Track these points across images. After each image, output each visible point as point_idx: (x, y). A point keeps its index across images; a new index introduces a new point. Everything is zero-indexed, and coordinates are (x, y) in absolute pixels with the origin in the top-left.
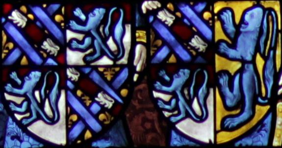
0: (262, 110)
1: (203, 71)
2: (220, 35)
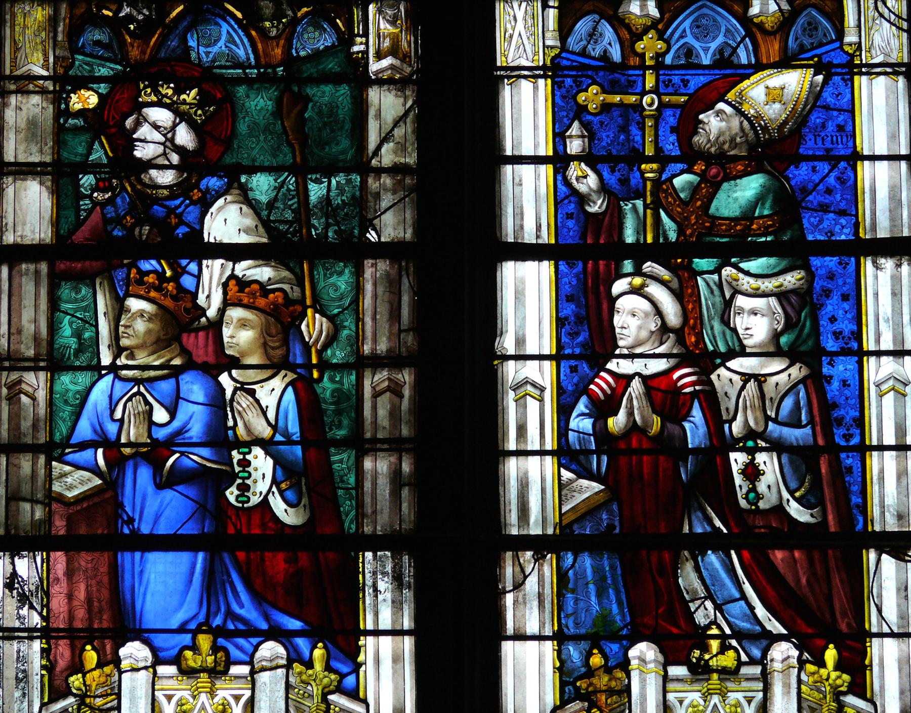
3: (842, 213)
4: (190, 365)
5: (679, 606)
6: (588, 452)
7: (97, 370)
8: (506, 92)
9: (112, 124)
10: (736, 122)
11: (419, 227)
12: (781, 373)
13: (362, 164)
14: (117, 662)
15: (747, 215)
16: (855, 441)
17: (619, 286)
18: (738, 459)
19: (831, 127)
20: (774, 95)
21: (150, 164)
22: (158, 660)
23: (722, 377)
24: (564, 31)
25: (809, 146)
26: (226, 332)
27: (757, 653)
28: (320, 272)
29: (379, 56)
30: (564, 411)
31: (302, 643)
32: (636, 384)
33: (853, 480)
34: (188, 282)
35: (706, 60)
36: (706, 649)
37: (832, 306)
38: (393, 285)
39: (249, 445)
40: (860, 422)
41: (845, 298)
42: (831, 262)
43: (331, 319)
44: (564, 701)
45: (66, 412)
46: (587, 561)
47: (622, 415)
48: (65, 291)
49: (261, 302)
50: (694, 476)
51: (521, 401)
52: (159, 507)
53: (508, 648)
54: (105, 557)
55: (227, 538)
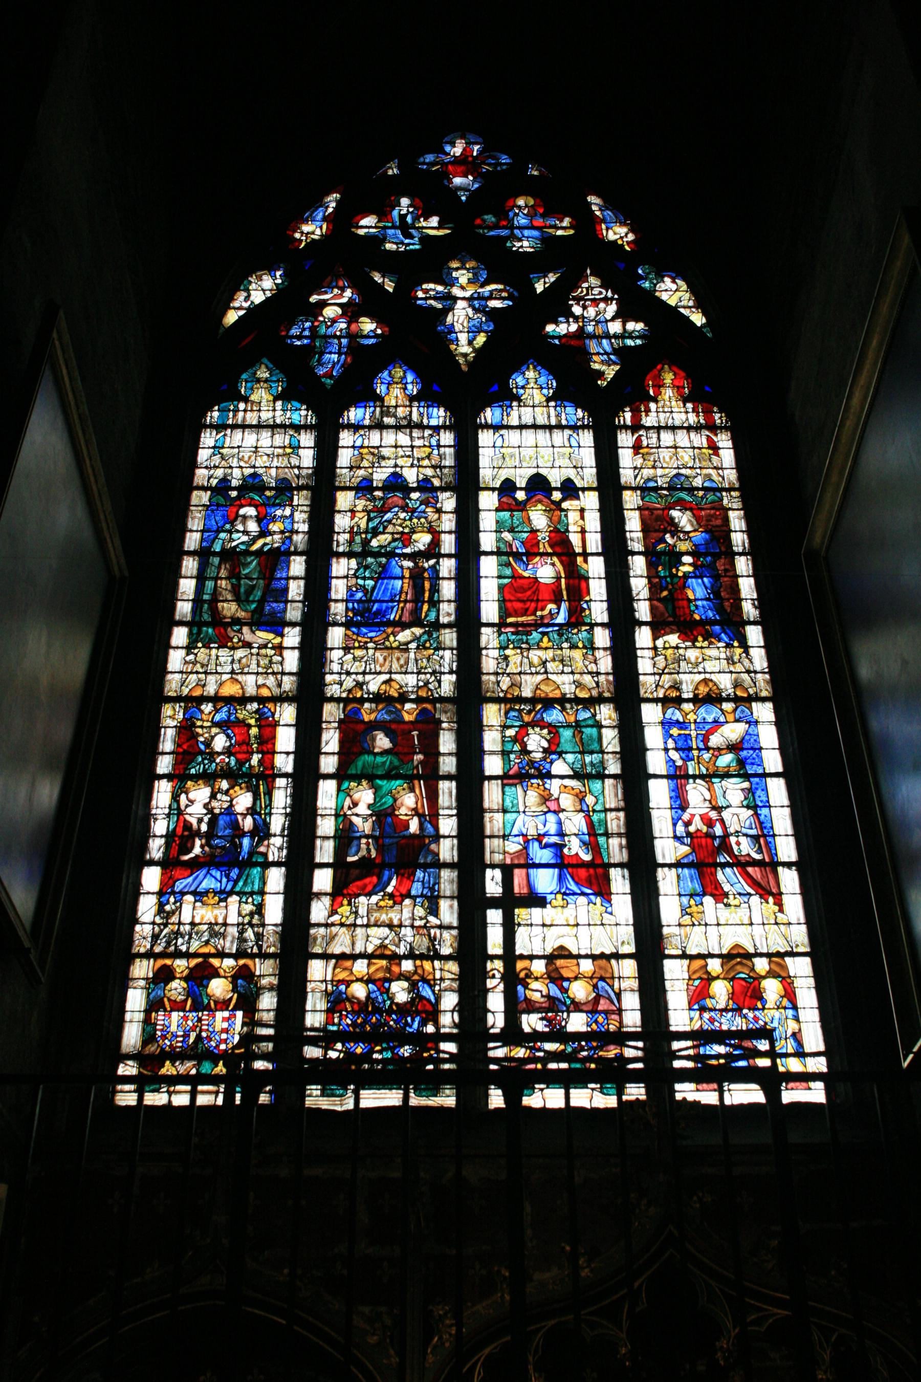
2: (767, 1020)
3: (759, 765)
4: (549, 811)
5: (718, 886)
7: (519, 812)
10: (722, 738)
11: (623, 769)
13: (602, 752)
15: (729, 766)
17: (688, 787)
18: (733, 840)
20: (733, 731)
23: (726, 814)
25: (746, 745)
28: (590, 783)
30: (675, 825)
31: (592, 897)
33: (772, 845)
34: (547, 786)
36: (728, 898)
37: (759, 793)
38: (616, 787)
40: (772, 828)
42: (757, 780)
45: (509, 826)
46: (686, 871)
48: (507, 789)
49: (572, 792)
50: (720, 845)
55: (563, 864)
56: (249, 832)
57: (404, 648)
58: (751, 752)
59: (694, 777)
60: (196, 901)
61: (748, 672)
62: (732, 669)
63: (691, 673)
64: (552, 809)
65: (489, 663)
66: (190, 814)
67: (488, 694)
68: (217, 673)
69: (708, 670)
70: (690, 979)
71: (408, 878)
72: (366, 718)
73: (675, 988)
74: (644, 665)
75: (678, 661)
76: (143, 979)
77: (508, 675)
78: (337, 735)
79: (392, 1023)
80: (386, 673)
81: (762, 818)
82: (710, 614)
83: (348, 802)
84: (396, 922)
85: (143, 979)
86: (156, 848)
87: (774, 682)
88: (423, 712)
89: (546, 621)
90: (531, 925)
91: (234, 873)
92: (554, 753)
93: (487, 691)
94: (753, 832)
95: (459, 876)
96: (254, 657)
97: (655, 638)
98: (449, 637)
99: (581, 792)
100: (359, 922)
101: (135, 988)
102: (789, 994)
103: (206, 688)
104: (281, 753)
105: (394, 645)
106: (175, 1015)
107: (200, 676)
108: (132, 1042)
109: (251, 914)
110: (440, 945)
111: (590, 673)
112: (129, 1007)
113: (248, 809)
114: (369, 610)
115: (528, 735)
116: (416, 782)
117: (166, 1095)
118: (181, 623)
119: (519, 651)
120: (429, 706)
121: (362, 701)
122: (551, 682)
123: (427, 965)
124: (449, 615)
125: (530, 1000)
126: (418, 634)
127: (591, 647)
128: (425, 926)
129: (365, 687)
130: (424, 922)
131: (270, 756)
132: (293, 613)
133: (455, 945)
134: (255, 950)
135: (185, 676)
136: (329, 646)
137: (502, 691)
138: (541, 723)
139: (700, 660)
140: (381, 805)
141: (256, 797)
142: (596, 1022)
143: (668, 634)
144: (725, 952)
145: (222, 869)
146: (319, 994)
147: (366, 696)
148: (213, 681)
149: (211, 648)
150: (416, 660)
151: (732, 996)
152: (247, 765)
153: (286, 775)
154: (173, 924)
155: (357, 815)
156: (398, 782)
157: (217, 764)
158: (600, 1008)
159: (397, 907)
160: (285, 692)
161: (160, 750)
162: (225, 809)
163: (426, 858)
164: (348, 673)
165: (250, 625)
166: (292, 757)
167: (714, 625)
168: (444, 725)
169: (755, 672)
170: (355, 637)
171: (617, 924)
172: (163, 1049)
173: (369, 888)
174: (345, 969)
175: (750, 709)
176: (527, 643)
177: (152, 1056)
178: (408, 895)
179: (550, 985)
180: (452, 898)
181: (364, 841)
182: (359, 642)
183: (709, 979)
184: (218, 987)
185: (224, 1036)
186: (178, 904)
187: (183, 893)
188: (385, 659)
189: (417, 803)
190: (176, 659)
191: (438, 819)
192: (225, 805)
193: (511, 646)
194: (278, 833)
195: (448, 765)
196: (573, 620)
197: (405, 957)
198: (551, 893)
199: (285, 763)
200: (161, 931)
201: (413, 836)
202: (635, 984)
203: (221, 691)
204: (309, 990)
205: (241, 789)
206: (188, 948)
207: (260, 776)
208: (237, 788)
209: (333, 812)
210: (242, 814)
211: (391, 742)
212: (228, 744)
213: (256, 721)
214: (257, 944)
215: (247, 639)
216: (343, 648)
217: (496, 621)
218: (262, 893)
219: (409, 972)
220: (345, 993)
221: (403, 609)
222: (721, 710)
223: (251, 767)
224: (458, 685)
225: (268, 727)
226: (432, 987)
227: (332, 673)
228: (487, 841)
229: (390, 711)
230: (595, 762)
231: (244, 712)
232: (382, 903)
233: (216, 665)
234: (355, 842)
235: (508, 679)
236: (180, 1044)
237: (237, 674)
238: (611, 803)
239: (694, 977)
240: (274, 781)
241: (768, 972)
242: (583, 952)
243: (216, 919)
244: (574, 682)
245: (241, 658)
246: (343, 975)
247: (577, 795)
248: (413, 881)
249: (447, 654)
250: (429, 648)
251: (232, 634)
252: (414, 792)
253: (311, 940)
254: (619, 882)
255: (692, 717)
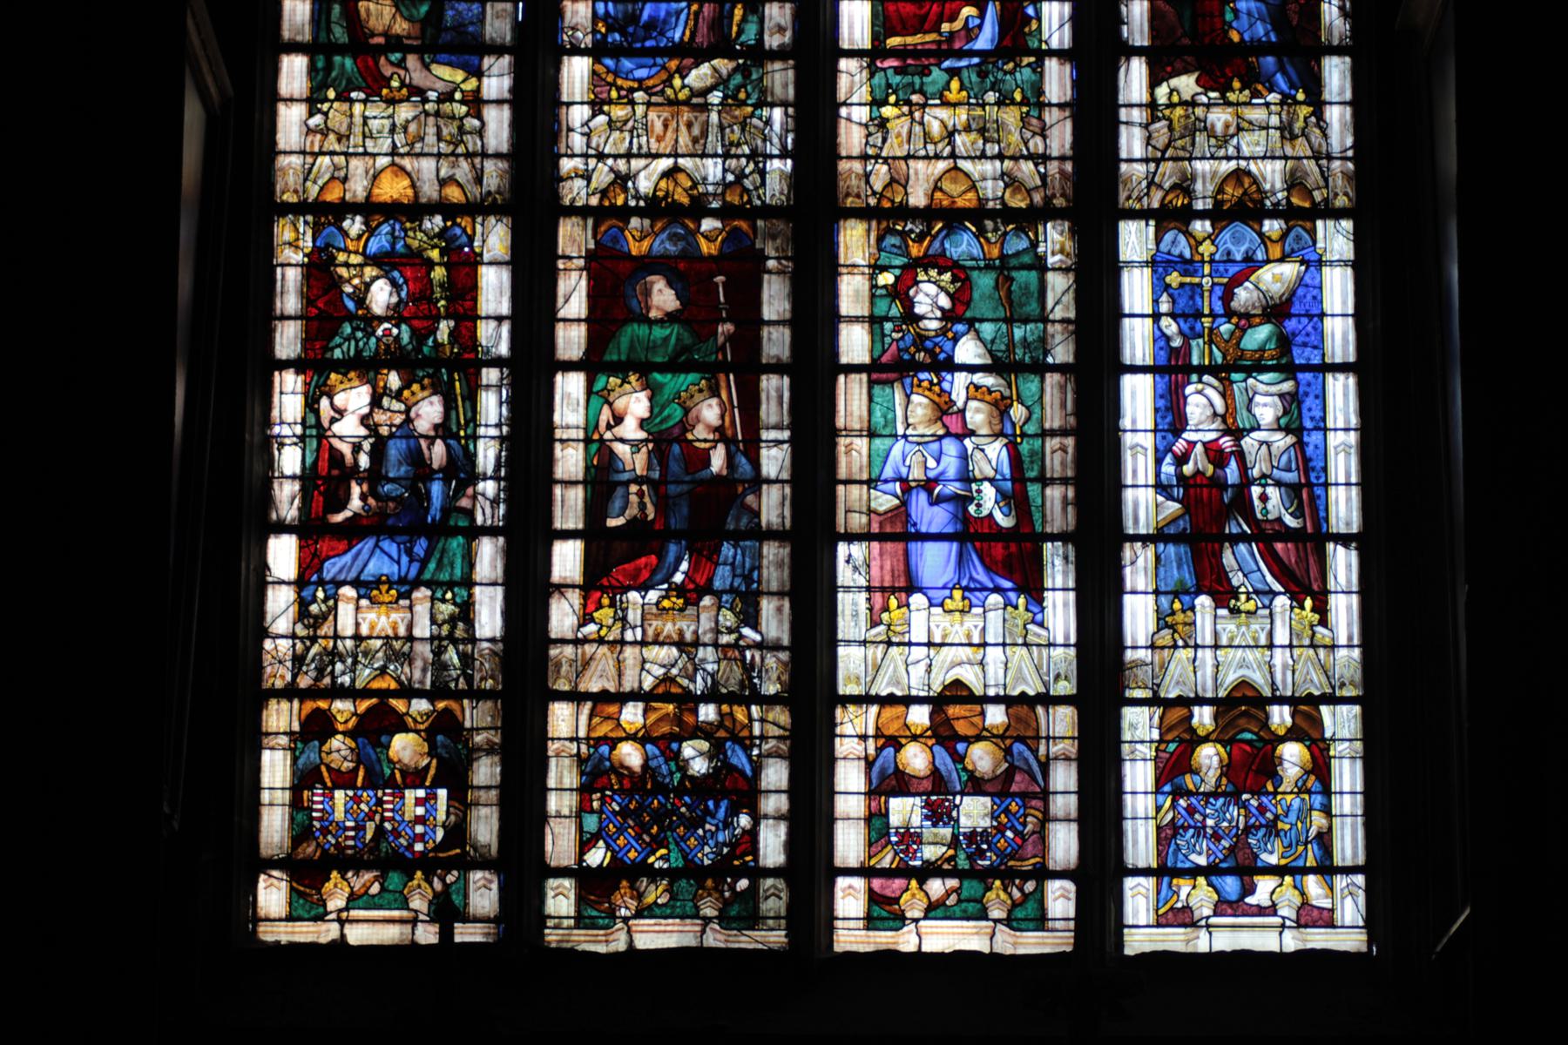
0: (1301, 848)
1: (1272, 829)
2: (1280, 811)
3: (1315, 347)
4: (948, 434)
5: (1222, 575)
6: (1171, 486)
7: (896, 436)
8: (1125, 276)
9: (901, 292)
10: (1255, 294)
11: (1077, 354)
12: (1281, 441)
13: (1044, 319)
14: (908, 605)
15: (1262, 350)
16: (1322, 480)
17: (1189, 390)
18: (1256, 491)
19: (1309, 297)
21: (922, 318)
22: (931, 605)
23: (1248, 443)
24: (1158, 240)
25: (1296, 308)
26: (968, 415)
27: (1267, 602)
28: (1020, 380)
29: (1053, 254)
30: (1159, 462)
31: (1012, 595)
32: (1199, 447)
33: (1321, 504)
34: (946, 386)
35: (1239, 257)
36: (1237, 599)
37: (1309, 402)
38: (1063, 389)
39: (982, 480)
40: (1325, 469)
41: (1317, 397)
43: (1028, 408)
44: (1159, 630)
45: (878, 462)
46: (1171, 549)
47: (1191, 463)
49: (988, 398)
50: (1232, 500)
51: (1134, 456)
52: (933, 518)
53: (1128, 600)
54: (900, 546)
55: (970, 534)
56: (441, 470)
57: (697, 102)
58: (1305, 320)
59: (1201, 370)
60: (360, 597)
61: (1317, 156)
62: (1289, 151)
63: (1213, 157)
64: (953, 430)
65: (851, 138)
66: (340, 438)
67: (849, 202)
68: (366, 154)
69: (1246, 151)
70: (1160, 742)
71: (709, 559)
72: (635, 249)
73: (1139, 755)
74: (1132, 142)
75: (1191, 131)
76: (285, 733)
77: (886, 160)
78: (584, 283)
79: (683, 810)
80: (668, 156)
81: (1310, 450)
82: (1260, 29)
83: (606, 415)
84: (689, 637)
85: (285, 733)
86: (287, 499)
87: (1359, 179)
88: (733, 235)
89: (957, 46)
90: (910, 644)
91: (420, 547)
92: (960, 320)
93: (848, 195)
94: (1291, 477)
95: (793, 555)
96: (431, 120)
97: (1154, 83)
98: (781, 78)
99: (1003, 398)
100: (629, 636)
101: (272, 749)
102: (1320, 768)
103: (351, 185)
104: (488, 318)
105: (681, 96)
106: (339, 795)
107: (336, 158)
108: (276, 838)
109: (452, 620)
110: (760, 677)
111: (1030, 157)
112: (266, 780)
113: (436, 427)
114: (634, 18)
115: (917, 283)
116: (722, 377)
117: (336, 926)
118: (294, 48)
119: (905, 109)
120: (744, 225)
121: (625, 213)
122: (961, 175)
123: (740, 714)
124: (781, 30)
125: (903, 773)
126: (724, 72)
127: (1035, 100)
128: (735, 645)
129: (630, 184)
130: (734, 636)
131: (469, 324)
132: (497, 23)
133: (785, 677)
134: (462, 684)
135: (309, 160)
136: (565, 98)
137: (874, 193)
138: (941, 261)
139: (1232, 130)
140: (662, 422)
141: (449, 405)
142: (1007, 811)
143: (1178, 74)
144: (1222, 694)
145: (399, 539)
146: (567, 761)
147: (632, 203)
148: (361, 171)
149: (352, 101)
150: (722, 128)
151: (1227, 770)
152: (430, 342)
153: (497, 362)
154: (325, 637)
155: (622, 441)
156: (692, 377)
157: (379, 340)
158: (1014, 788)
159: (691, 610)
160: (489, 193)
161: (278, 312)
162: (399, 427)
163: (738, 519)
164: (601, 157)
165: (419, 51)
166: (505, 329)
167: (1266, 54)
168: (771, 264)
169: (1330, 158)
170: (610, 78)
171: (1050, 645)
172: (325, 852)
173: (645, 574)
174: (608, 718)
175: (1312, 233)
176: (922, 92)
177: (308, 861)
178: (708, 589)
179: (937, 749)
180: (780, 594)
181: (634, 488)
182: (619, 89)
183: (1194, 741)
184: (404, 747)
185: (419, 829)
186: (331, 603)
187: (339, 584)
188: (666, 126)
189: (722, 417)
190: (291, 122)
191: (759, 448)
192: (398, 419)
193: (892, 99)
194: (490, 472)
195: (776, 344)
196: (1007, 42)
197: (706, 698)
198: (944, 588)
199: (495, 338)
200: (308, 649)
201: (719, 476)
202: (1071, 748)
203: (376, 191)
204: (550, 753)
205: (423, 388)
206: (353, 681)
207: (454, 364)
208: (415, 387)
209: (581, 435)
210: (426, 437)
211: (678, 297)
212: (395, 299)
213: (442, 255)
214: (464, 673)
215: (415, 82)
216: (592, 103)
217: (867, 45)
218: (469, 583)
219: (711, 724)
220: (609, 759)
221: (697, 14)
222: (1261, 234)
223: (437, 345)
224: (796, 180)
225: (465, 266)
226: (747, 749)
227: (573, 156)
228: (841, 489)
229: (675, 234)
230: (1030, 339)
231: (420, 235)
232: (666, 603)
233: (364, 137)
234: (620, 491)
235: (885, 168)
236: (351, 843)
237: (402, 155)
238: (1054, 420)
239: (1169, 737)
240: (479, 374)
241: (1289, 730)
242: (991, 692)
243: (395, 628)
244: (1003, 174)
245: (408, 122)
246: (603, 730)
247: (995, 404)
248: (717, 564)
249: (777, 113)
250: (743, 103)
251: (387, 71)
252: (719, 396)
253: (551, 668)
254: (1058, 570)
255: (1206, 249)
